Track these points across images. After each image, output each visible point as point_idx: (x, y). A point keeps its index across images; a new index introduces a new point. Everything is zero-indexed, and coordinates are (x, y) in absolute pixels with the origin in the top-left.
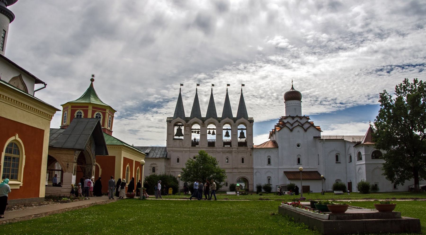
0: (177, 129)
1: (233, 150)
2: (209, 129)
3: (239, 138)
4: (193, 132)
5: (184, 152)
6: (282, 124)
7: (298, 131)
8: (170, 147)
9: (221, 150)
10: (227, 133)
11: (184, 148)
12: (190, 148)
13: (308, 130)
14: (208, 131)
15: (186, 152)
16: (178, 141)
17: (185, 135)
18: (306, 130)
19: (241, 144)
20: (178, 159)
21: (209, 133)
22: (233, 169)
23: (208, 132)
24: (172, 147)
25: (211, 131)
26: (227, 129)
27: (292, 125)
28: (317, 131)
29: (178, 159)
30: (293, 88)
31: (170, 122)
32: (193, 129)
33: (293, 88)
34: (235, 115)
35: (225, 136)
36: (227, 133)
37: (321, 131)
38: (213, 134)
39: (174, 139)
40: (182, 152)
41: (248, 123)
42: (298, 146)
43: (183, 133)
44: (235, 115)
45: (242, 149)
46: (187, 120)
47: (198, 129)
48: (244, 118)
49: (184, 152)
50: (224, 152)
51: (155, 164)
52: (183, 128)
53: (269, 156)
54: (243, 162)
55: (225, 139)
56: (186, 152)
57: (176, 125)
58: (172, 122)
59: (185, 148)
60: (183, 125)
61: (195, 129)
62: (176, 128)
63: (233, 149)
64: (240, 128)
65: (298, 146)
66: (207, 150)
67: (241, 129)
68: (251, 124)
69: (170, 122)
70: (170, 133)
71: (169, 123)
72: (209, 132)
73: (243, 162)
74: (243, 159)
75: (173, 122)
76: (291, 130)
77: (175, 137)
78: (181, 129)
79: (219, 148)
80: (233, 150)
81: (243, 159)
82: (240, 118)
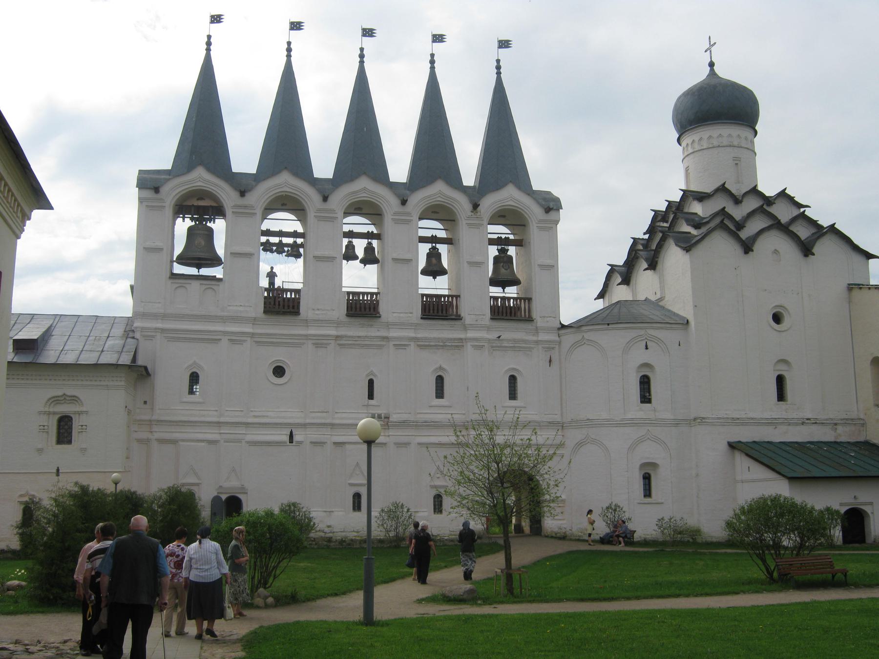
0: (190, 229)
1: (471, 334)
2: (350, 235)
4: (267, 247)
5: (225, 340)
6: (670, 228)
7: (776, 252)
8: (155, 316)
9: (412, 334)
10: (434, 255)
11: (223, 320)
12: (254, 321)
14: (345, 241)
15: (235, 339)
16: (196, 284)
17: (233, 255)
19: (502, 312)
20: (194, 378)
21: (350, 255)
24: (164, 317)
25: (360, 245)
26: (434, 240)
27: (740, 226)
29: (194, 378)
30: (712, 73)
31: (157, 190)
32: (268, 233)
33: (712, 73)
34: (469, 175)
35: (425, 272)
36: (434, 255)
37: (869, 256)
38: (370, 258)
39: (174, 276)
40: (212, 339)
41: (534, 211)
42: (777, 318)
43: (220, 251)
44: (469, 175)
45: (511, 332)
46: (242, 185)
47: (295, 234)
48: (519, 188)
50: (424, 345)
51: (74, 399)
52: (219, 226)
53: (646, 365)
55: (430, 286)
56: (235, 339)
57: (181, 210)
58: (165, 190)
60: (218, 211)
61: (281, 234)
62: (182, 226)
63: (465, 328)
64: (495, 236)
65: (777, 318)
66: (342, 332)
68: (552, 215)
69: (157, 190)
70: (150, 247)
71: (149, 194)
72: (350, 247)
75: (172, 192)
76: (747, 247)
77: (179, 269)
78: (211, 231)
79: (401, 325)
80: (471, 334)
82: (498, 186)
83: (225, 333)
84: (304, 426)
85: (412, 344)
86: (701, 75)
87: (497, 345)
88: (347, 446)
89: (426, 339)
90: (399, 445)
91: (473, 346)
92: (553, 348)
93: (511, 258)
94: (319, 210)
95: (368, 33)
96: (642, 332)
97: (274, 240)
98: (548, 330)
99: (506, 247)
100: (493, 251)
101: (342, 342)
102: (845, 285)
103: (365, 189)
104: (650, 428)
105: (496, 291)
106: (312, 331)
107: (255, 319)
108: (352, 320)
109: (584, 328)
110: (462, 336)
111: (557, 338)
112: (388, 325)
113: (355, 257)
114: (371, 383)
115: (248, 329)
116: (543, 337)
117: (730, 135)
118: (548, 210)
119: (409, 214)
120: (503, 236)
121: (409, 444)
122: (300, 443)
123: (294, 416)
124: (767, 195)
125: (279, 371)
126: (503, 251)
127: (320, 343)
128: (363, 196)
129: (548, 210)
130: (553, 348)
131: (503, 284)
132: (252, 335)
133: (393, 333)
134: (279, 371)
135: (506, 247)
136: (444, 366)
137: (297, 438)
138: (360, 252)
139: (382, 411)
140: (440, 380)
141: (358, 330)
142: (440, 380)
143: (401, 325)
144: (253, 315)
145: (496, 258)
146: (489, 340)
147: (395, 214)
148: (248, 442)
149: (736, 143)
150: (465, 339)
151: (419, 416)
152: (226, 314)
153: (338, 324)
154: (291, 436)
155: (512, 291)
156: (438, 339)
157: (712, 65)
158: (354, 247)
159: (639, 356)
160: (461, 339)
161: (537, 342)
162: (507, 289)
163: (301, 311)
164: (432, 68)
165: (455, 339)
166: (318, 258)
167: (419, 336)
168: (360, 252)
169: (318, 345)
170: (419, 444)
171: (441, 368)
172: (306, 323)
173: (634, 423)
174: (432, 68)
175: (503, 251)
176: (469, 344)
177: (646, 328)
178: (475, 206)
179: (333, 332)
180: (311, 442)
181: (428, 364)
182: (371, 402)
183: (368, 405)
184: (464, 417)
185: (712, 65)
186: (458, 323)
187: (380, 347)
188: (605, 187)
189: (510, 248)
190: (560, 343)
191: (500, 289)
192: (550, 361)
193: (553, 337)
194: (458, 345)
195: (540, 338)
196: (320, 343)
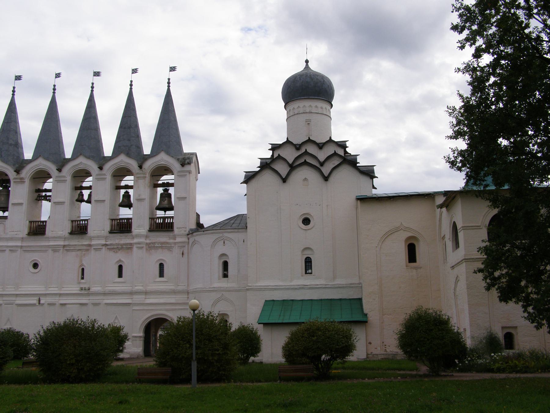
1: (136, 241)
3: (159, 208)
5: (8, 250)
7: (305, 179)
9: (103, 242)
11: (8, 239)
12: (22, 239)
13: (331, 179)
15: (13, 250)
18: (326, 179)
22: (131, 293)
23: (77, 197)
26: (127, 187)
28: (365, 180)
30: (307, 67)
33: (307, 67)
35: (122, 205)
42: (306, 221)
45: (162, 237)
49: (7, 251)
53: (223, 255)
54: (161, 274)
56: (13, 250)
59: (12, 239)
65: (306, 221)
66: (66, 243)
67: (163, 185)
68: (187, 168)
72: (82, 195)
73: (161, 274)
74: (161, 266)
79: (98, 237)
80: (136, 241)
81: (161, 266)
83: (7, 246)
84: (45, 295)
85: (104, 247)
86: (299, 68)
87: (151, 247)
88: (68, 306)
89: (111, 245)
90: (95, 304)
91: (137, 247)
92: (184, 246)
93: (170, 195)
94: (57, 177)
95: (97, 74)
96: (221, 235)
97: (44, 194)
98: (181, 236)
99: (168, 188)
100: (160, 190)
101: (68, 248)
102: (355, 197)
103: (81, 163)
104: (224, 293)
105: (160, 213)
106: (52, 243)
107: (23, 238)
108: (72, 236)
109: (195, 234)
110: (132, 242)
111: (187, 240)
112: (91, 239)
113: (83, 201)
114: (83, 270)
115: (19, 244)
116: (178, 240)
117: (310, 106)
118: (183, 165)
119: (105, 175)
120: (166, 182)
121: (99, 304)
122: (43, 304)
123: (39, 289)
124: (336, 141)
125: (35, 266)
126: (166, 191)
127: (55, 249)
128: (81, 167)
129: (183, 165)
130: (184, 246)
131: (165, 210)
132: (21, 247)
133: (93, 243)
134: (35, 266)
135: (168, 188)
136: (122, 259)
137: (42, 302)
138: (86, 198)
139: (86, 286)
140: (120, 267)
141: (76, 241)
142: (120, 267)
143: (98, 237)
144: (22, 236)
145: (161, 194)
146: (147, 243)
147: (97, 175)
148: (16, 305)
149: (308, 111)
150: (133, 243)
151: (107, 288)
152: (8, 236)
153: (65, 239)
154: (39, 300)
155: (170, 213)
156: (118, 244)
157: (307, 62)
158: (83, 195)
159: (220, 249)
160: (131, 244)
161: (175, 243)
162: (168, 212)
163: (47, 232)
164: (131, 89)
165: (128, 244)
166: (56, 203)
167: (108, 243)
168: (86, 198)
169: (55, 251)
170: (106, 304)
171: (120, 261)
172: (49, 239)
173: (215, 290)
174: (131, 89)
175: (166, 191)
176: (135, 246)
177: (222, 233)
178: (141, 167)
179: (62, 243)
180: (48, 304)
181: (113, 259)
182: (83, 281)
183: (80, 283)
184: (131, 288)
185: (307, 62)
186: (129, 234)
187: (87, 250)
188: (230, 146)
189: (170, 188)
190: (189, 242)
191: (163, 212)
192: (183, 254)
193: (185, 239)
194: (129, 248)
195: (176, 241)
196: (55, 249)
